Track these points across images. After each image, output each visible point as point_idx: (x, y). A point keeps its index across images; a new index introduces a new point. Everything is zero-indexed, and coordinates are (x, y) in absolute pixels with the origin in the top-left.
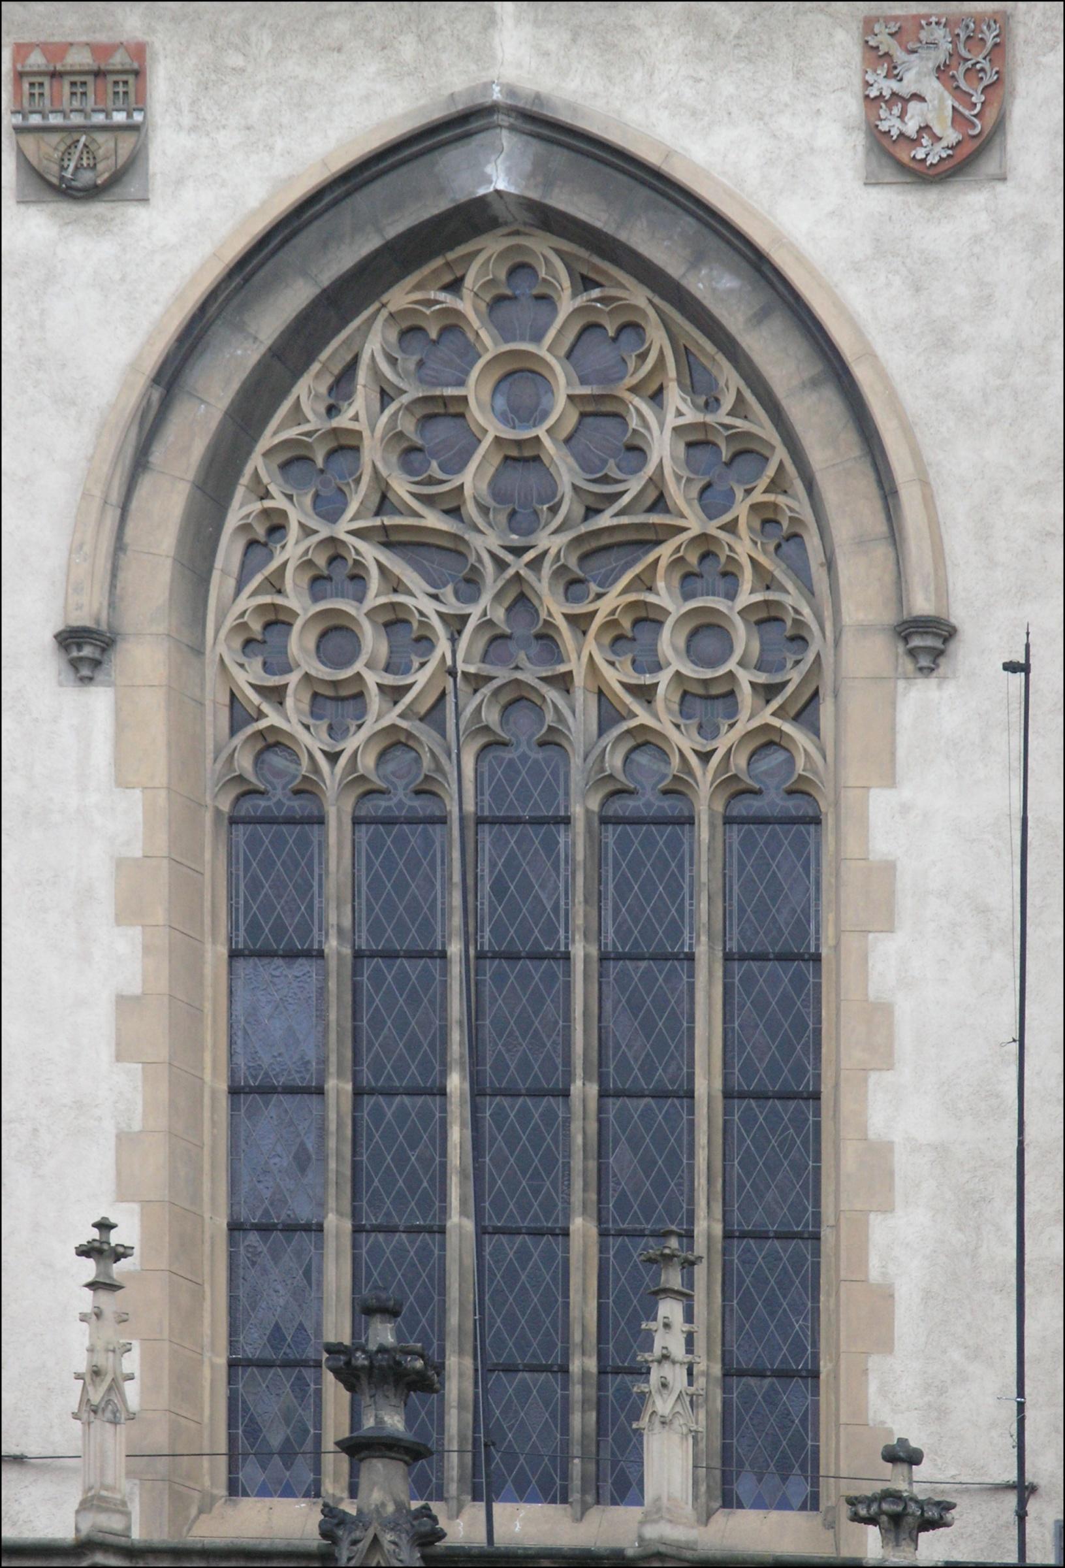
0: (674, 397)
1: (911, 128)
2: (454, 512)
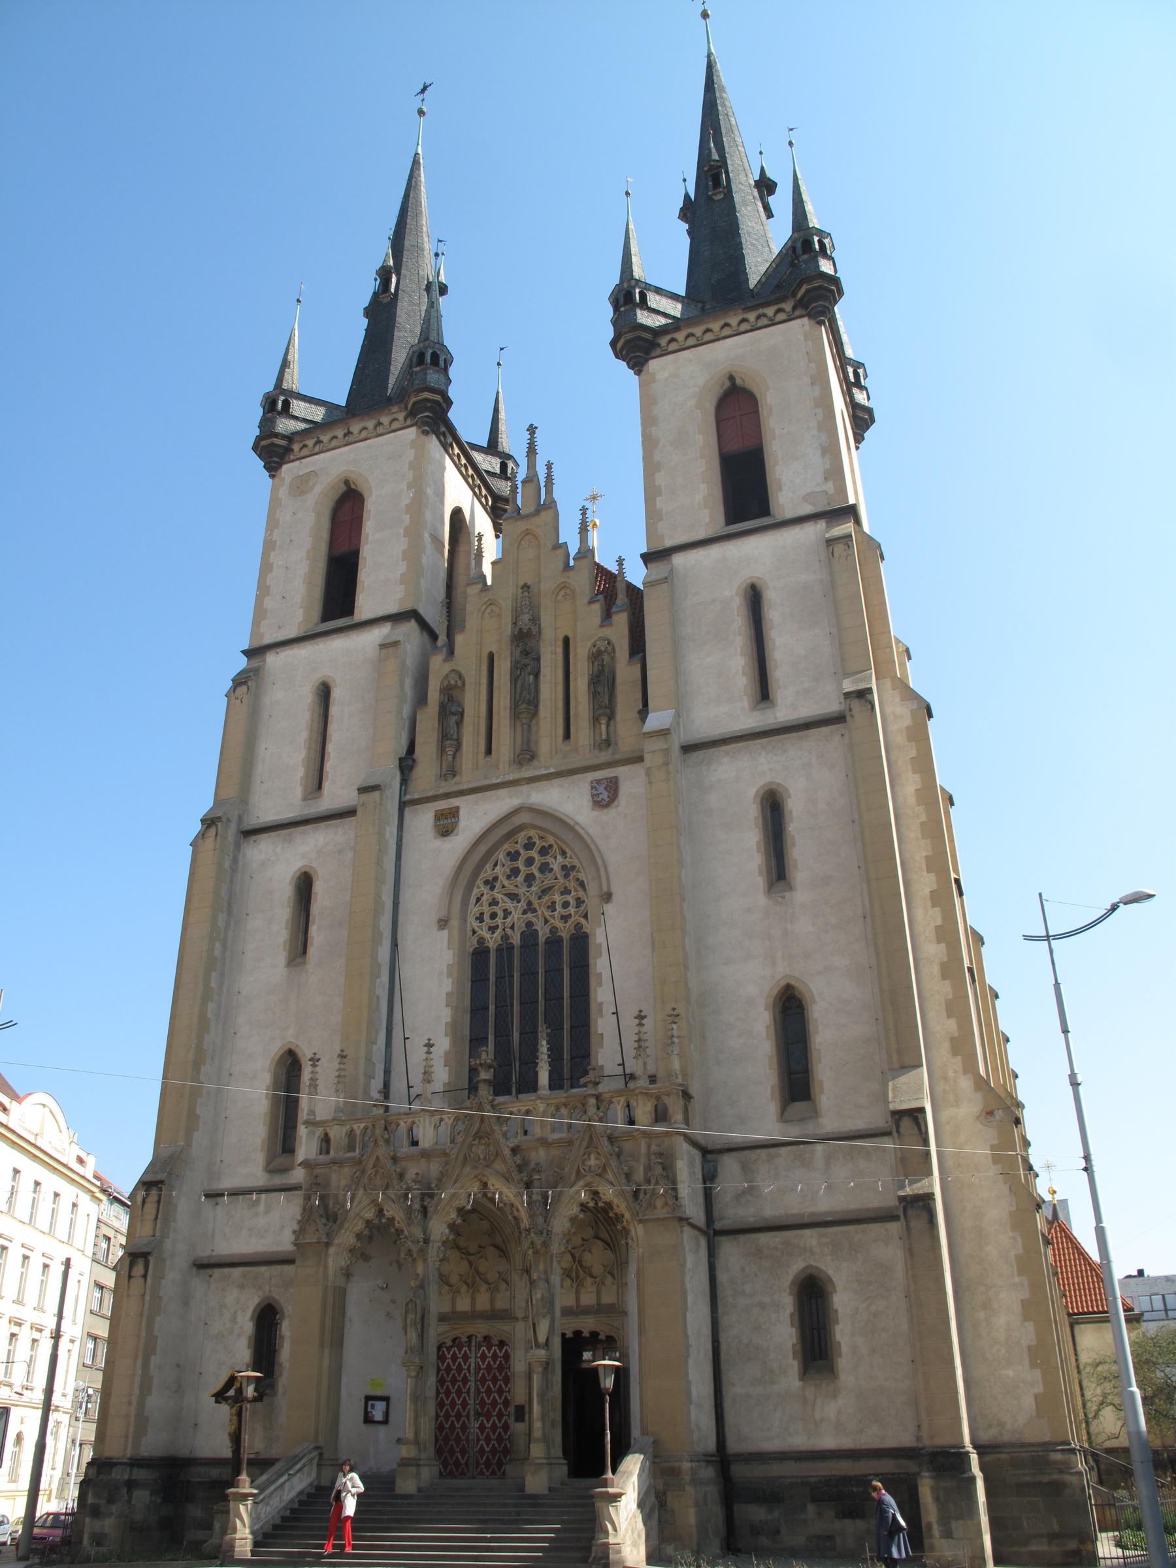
0: (559, 857)
1: (600, 799)
2: (516, 886)
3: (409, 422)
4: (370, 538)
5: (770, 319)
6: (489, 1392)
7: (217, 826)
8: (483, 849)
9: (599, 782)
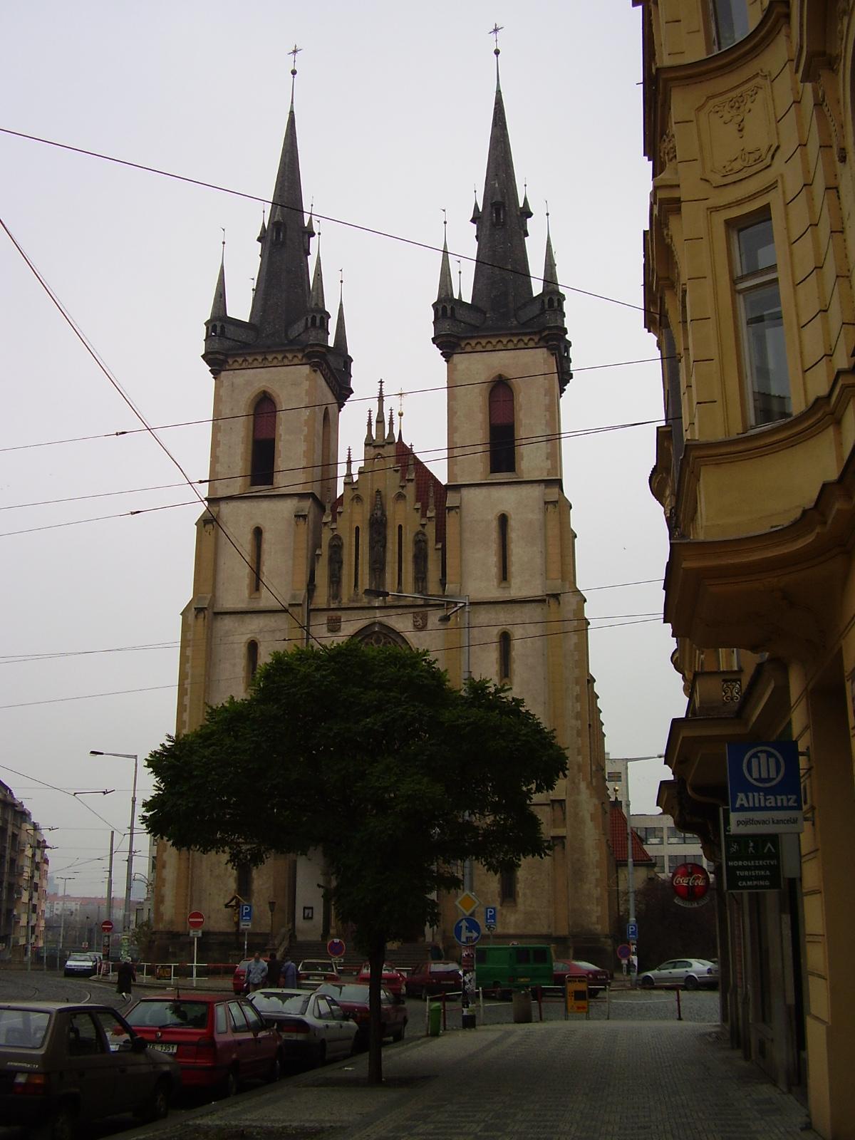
3: (304, 361)
4: (282, 438)
7: (204, 612)
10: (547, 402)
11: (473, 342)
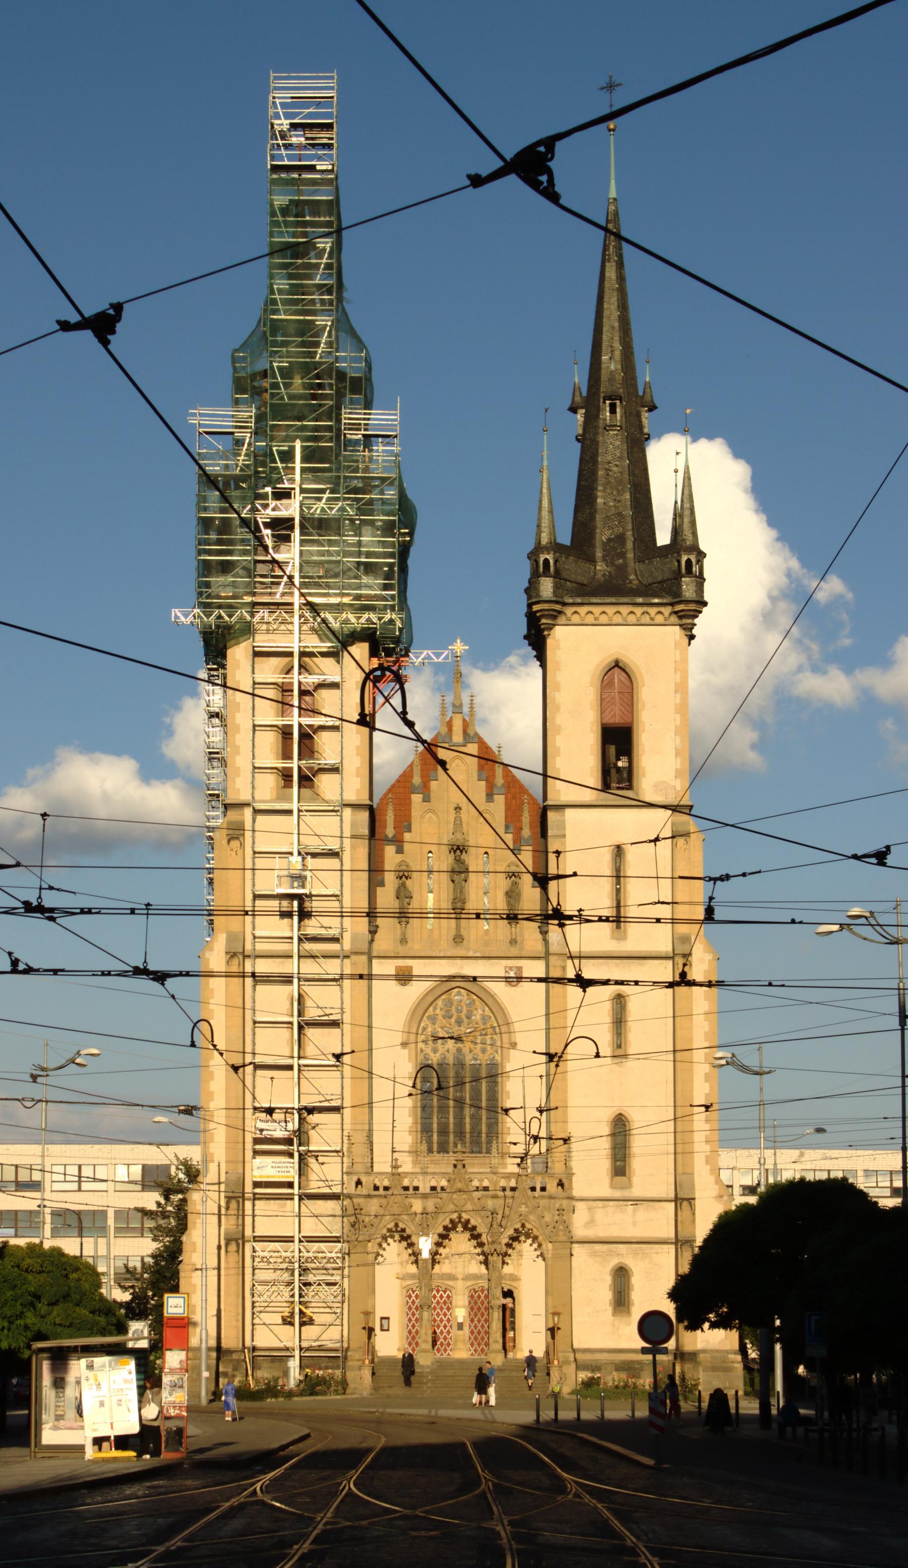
5: (652, 619)
6: (438, 1315)
8: (430, 999)
9: (511, 968)
10: (678, 701)
11: (583, 610)
